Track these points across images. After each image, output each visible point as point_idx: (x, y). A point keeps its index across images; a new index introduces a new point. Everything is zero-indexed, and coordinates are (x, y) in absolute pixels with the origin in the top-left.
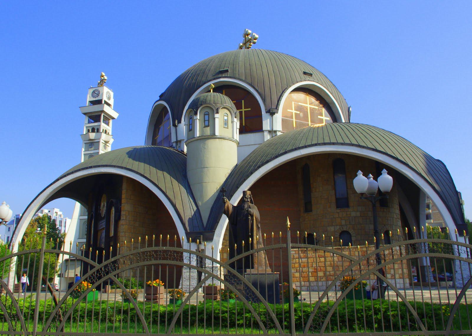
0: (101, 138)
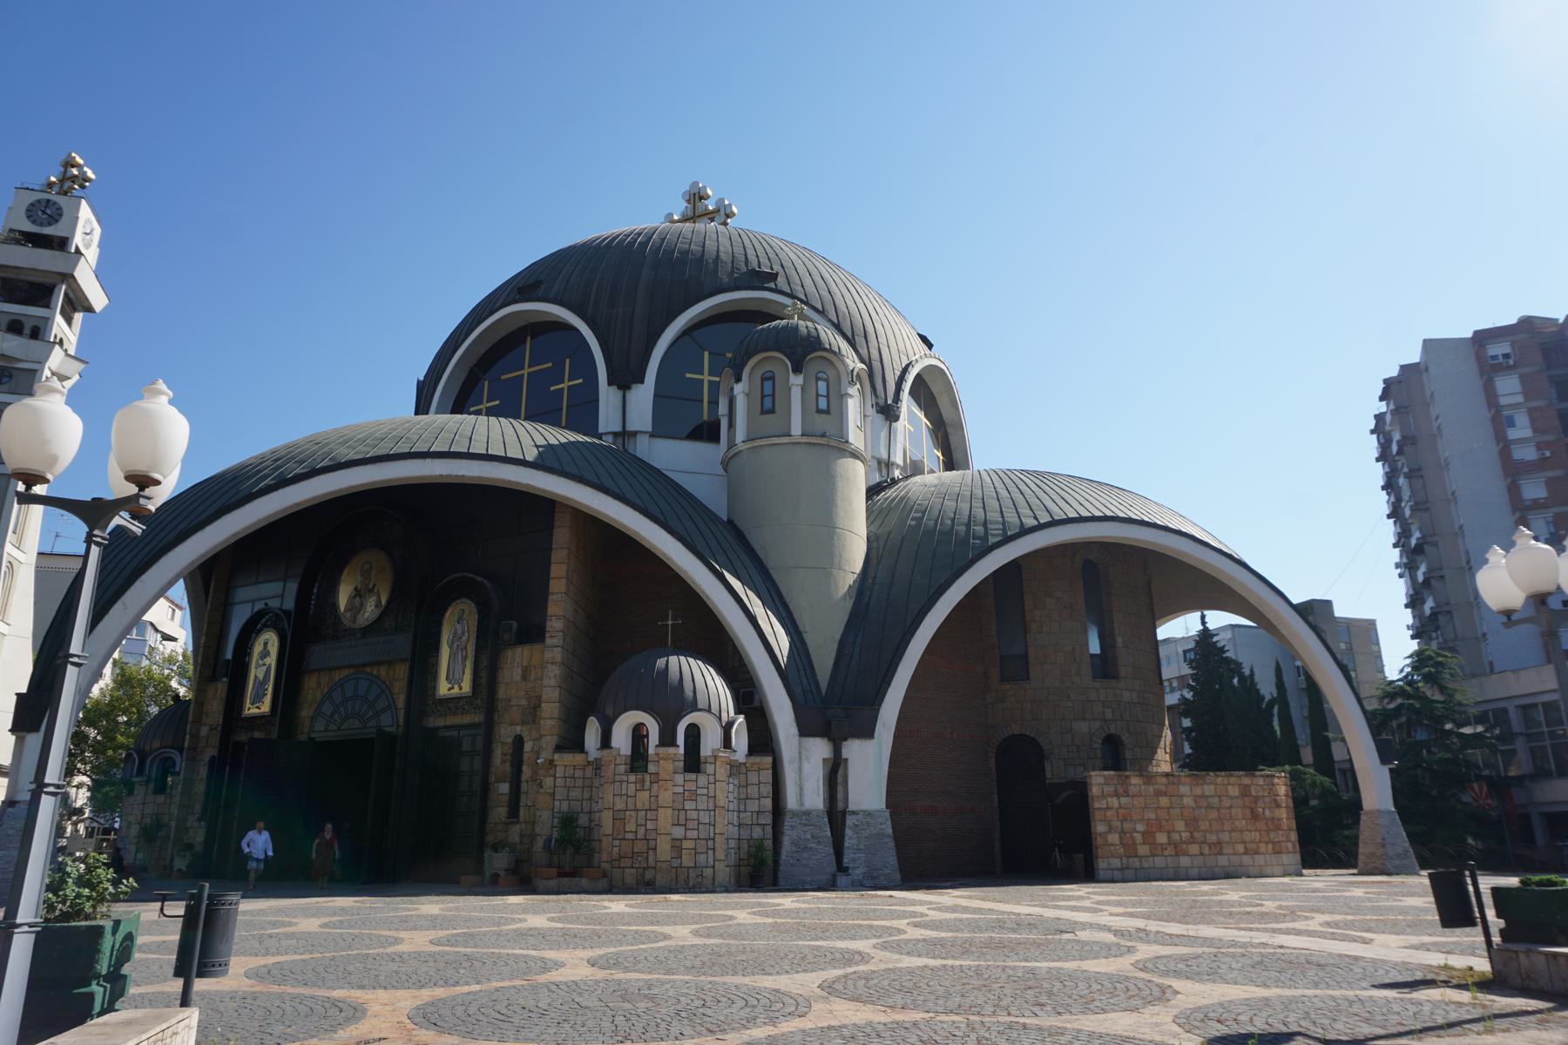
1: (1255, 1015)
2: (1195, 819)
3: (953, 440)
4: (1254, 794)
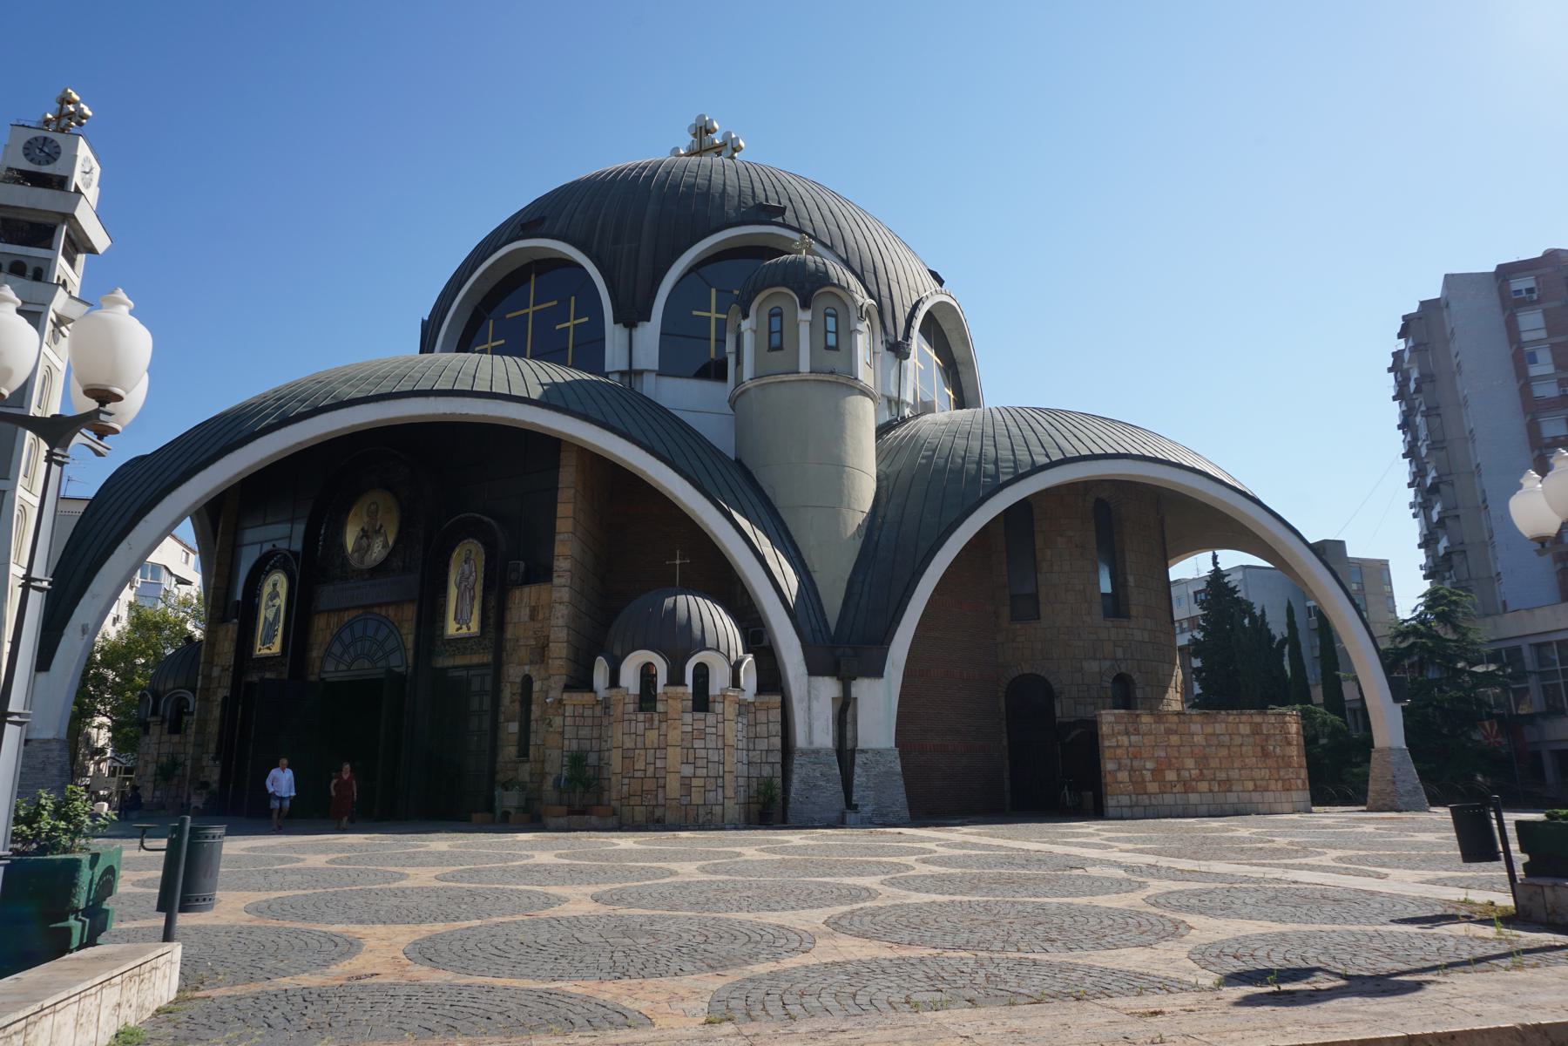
0: (51, 303)
1: (1272, 950)
2: (1205, 757)
3: (964, 379)
4: (1265, 732)
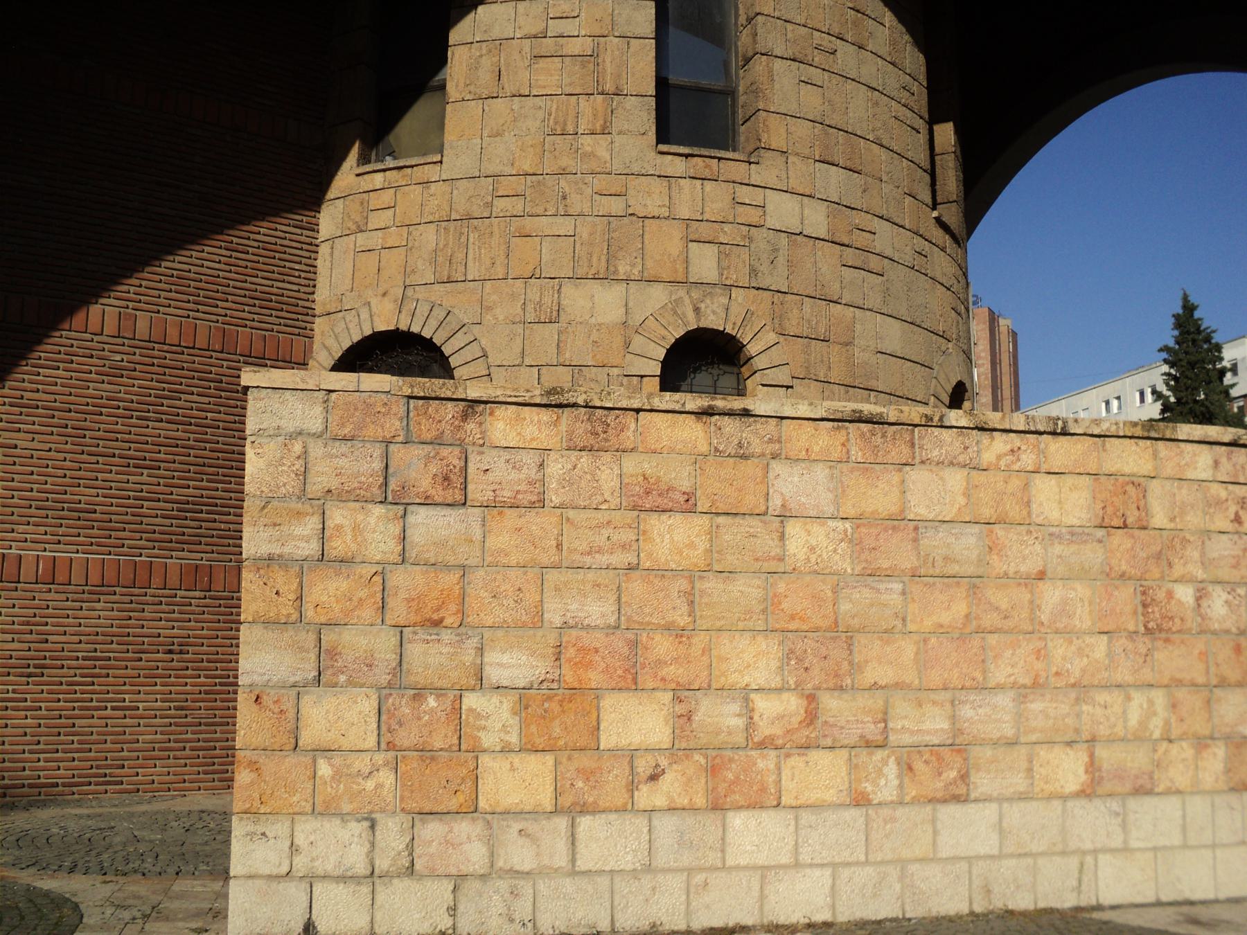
4: (1159, 518)
